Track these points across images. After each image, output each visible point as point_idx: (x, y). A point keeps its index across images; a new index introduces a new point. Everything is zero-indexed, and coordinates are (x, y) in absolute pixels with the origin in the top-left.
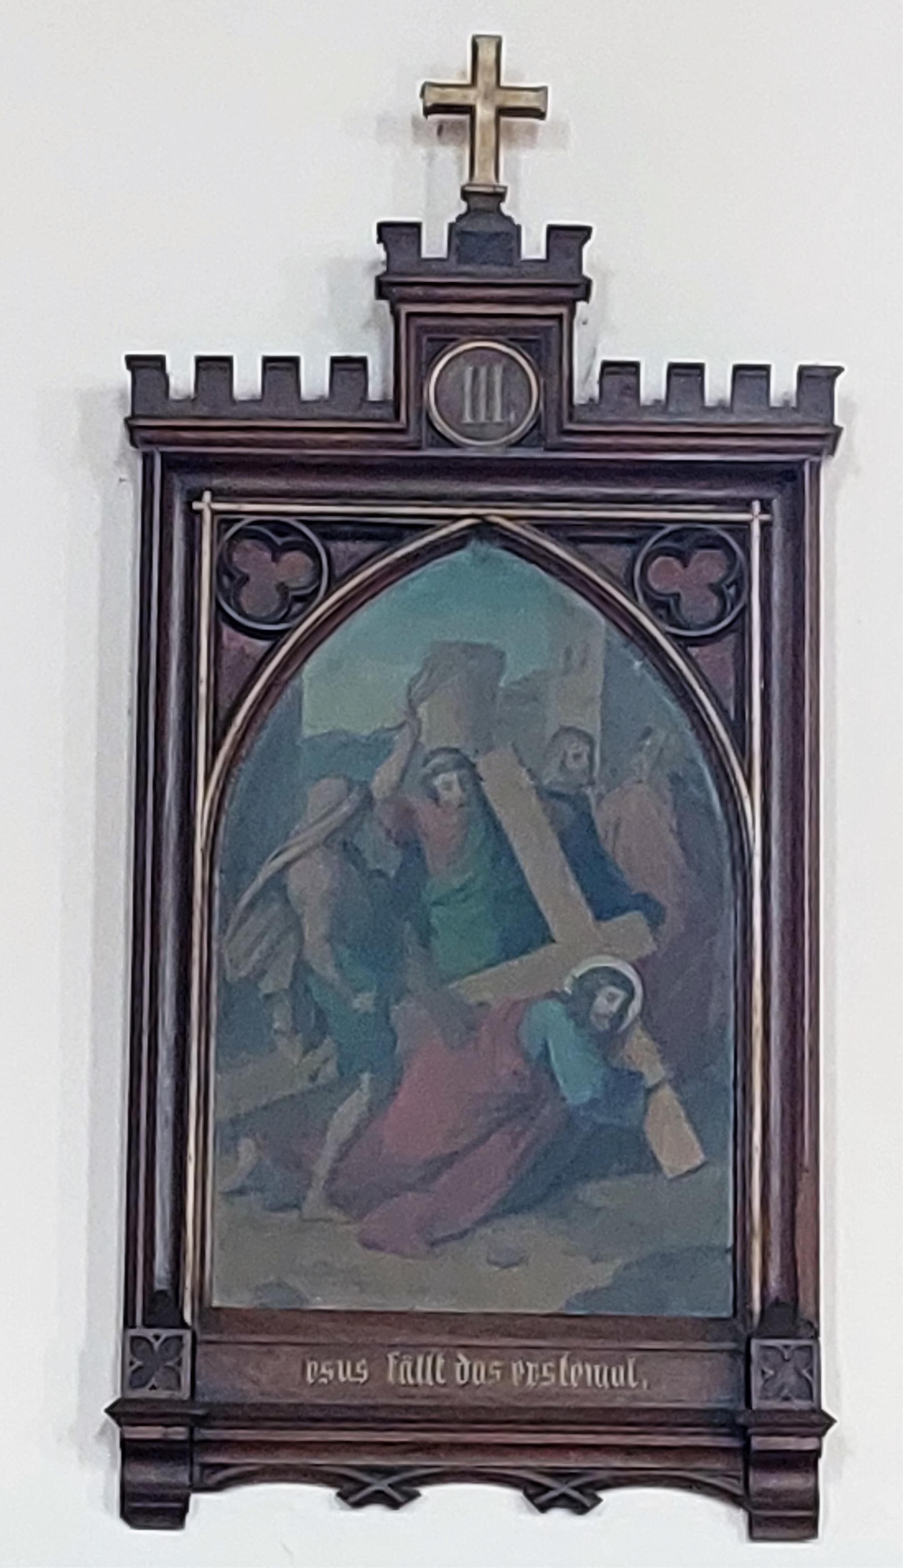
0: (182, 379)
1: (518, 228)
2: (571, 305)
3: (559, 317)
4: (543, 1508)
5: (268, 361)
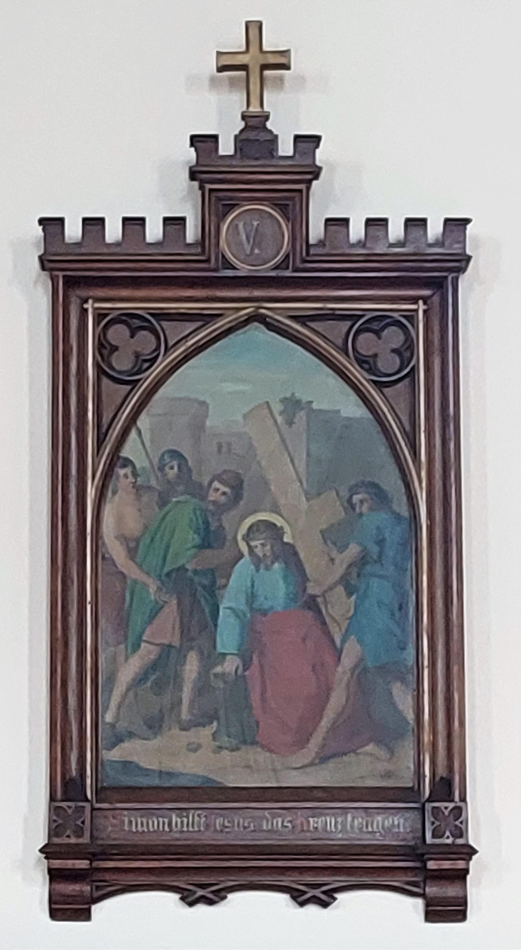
1: (276, 137)
2: (309, 182)
3: (300, 191)
4: (302, 904)
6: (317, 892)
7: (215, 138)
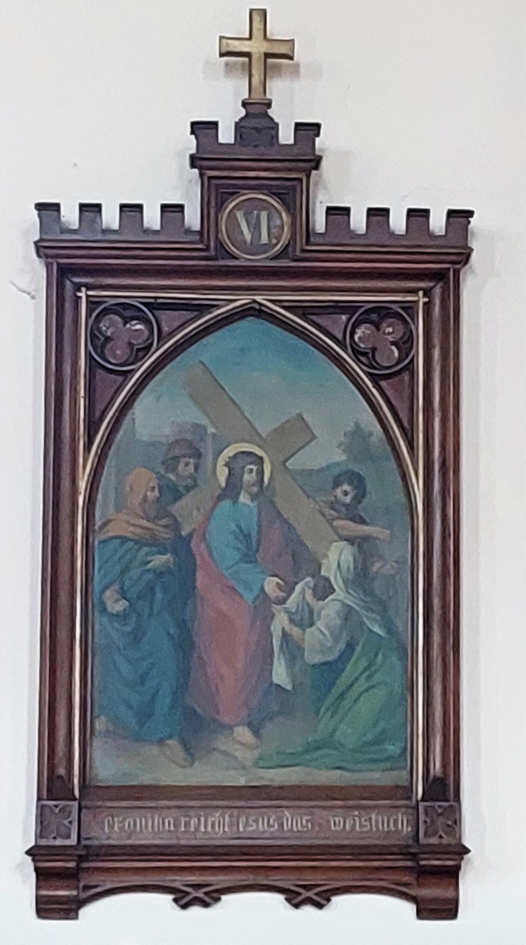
0: (70, 216)
7: (215, 125)
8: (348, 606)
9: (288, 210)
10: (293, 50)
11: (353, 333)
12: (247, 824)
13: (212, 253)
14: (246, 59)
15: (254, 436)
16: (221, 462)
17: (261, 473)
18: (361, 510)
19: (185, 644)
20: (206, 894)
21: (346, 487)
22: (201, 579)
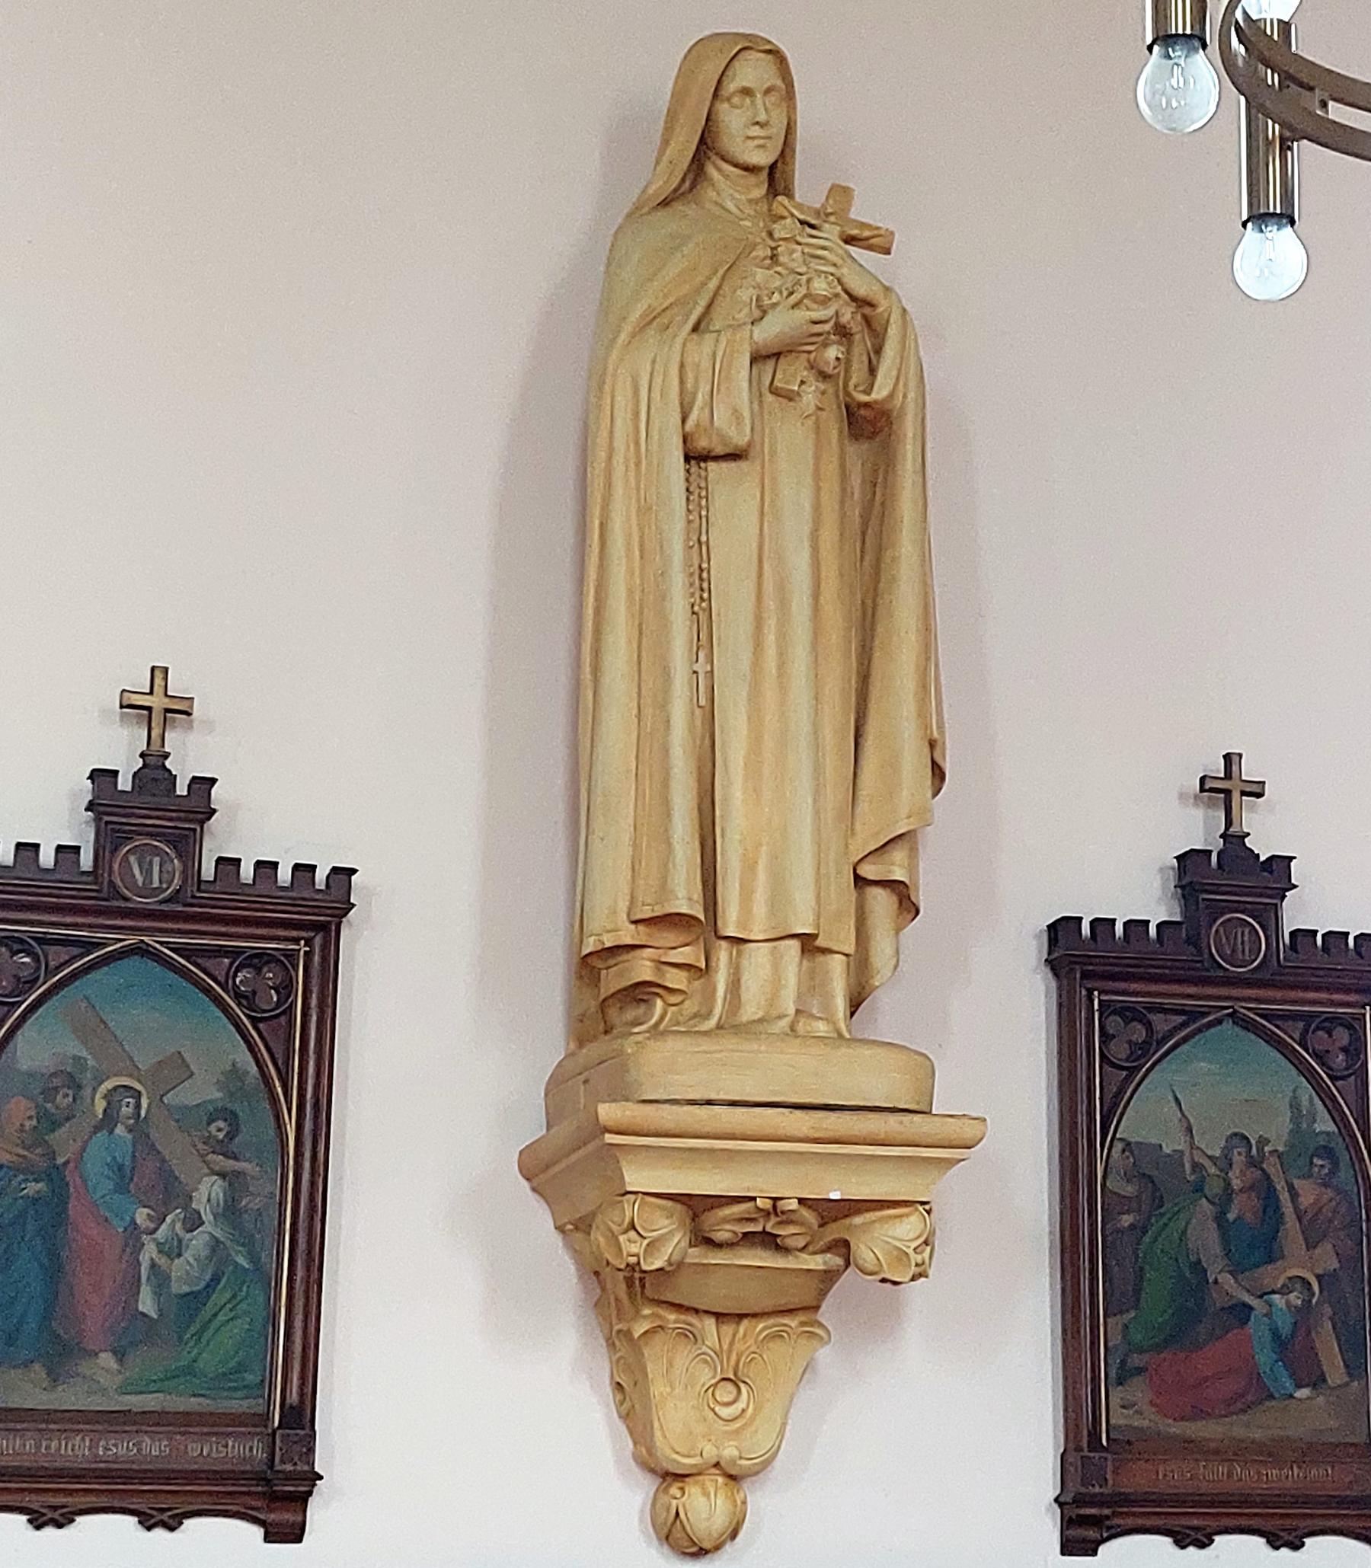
2: (202, 823)
5: (19, 845)
6: (165, 1517)
8: (217, 1240)
9: (180, 856)
10: (192, 707)
11: (235, 976)
12: (106, 1449)
13: (104, 894)
14: (145, 712)
15: (134, 1072)
16: (98, 1096)
17: (138, 1106)
18: (233, 1147)
19: (55, 1270)
20: (62, 1515)
21: (221, 1124)
22: (74, 1208)
